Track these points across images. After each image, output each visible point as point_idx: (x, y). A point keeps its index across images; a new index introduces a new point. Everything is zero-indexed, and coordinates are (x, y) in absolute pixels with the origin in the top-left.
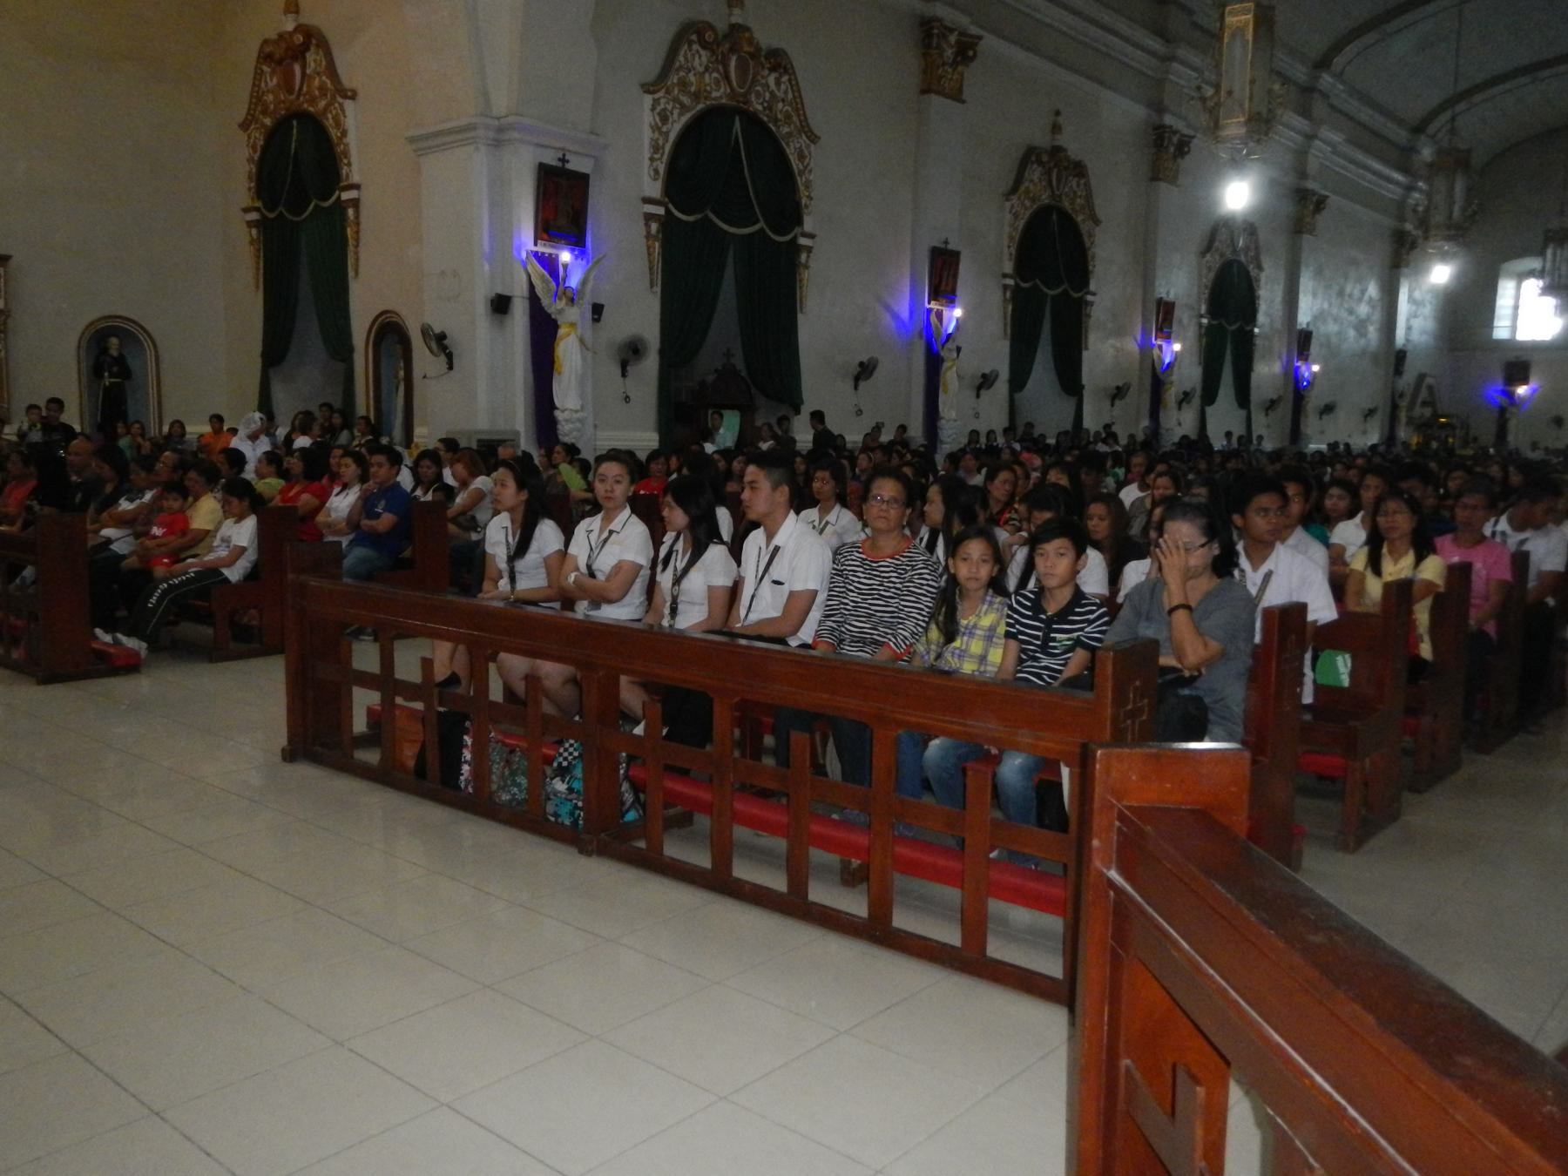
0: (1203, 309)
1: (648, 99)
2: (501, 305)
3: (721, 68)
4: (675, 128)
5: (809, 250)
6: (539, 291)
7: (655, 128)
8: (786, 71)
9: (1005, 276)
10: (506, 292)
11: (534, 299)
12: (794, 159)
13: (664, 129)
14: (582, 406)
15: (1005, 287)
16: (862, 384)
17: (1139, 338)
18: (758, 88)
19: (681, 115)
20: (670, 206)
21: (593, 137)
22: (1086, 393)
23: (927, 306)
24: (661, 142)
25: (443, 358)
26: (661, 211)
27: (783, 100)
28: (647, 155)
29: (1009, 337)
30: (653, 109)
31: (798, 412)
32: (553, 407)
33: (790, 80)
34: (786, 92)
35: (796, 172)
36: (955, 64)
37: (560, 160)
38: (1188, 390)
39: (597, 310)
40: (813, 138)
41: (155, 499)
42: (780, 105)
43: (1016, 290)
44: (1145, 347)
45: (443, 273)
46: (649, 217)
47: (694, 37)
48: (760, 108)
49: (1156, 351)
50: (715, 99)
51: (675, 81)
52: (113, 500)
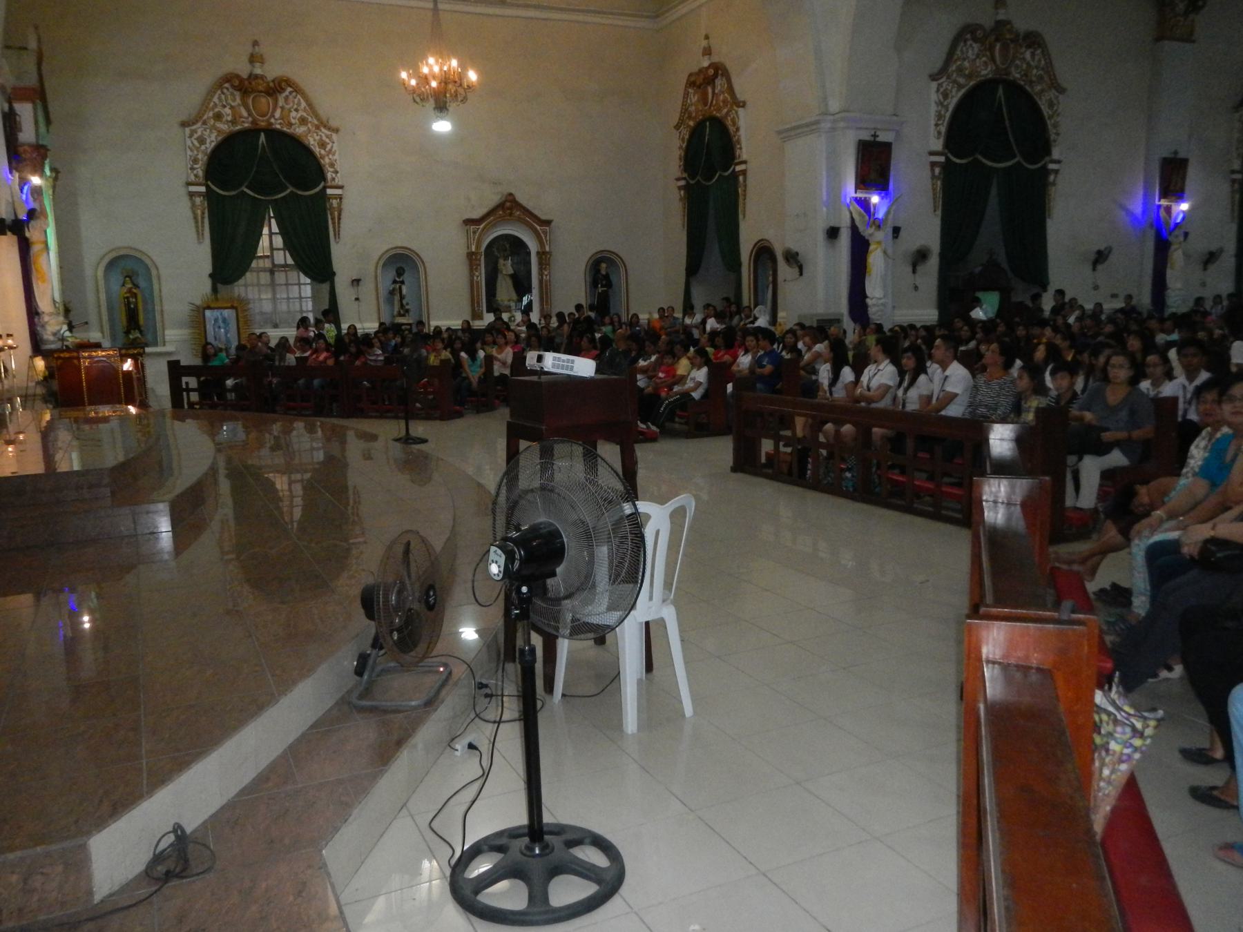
1: (934, 85)
2: (833, 233)
3: (988, 53)
4: (953, 102)
6: (858, 223)
7: (940, 103)
8: (1039, 46)
9: (1233, 172)
10: (837, 225)
11: (854, 228)
13: (945, 103)
14: (884, 296)
15: (1234, 181)
19: (958, 90)
20: (949, 155)
21: (895, 118)
23: (1157, 203)
24: (943, 112)
25: (797, 270)
26: (942, 159)
27: (1037, 67)
28: (933, 122)
30: (938, 90)
31: (1045, 290)
32: (865, 296)
33: (1043, 52)
34: (1040, 61)
35: (1047, 118)
36: (1186, 14)
37: (872, 136)
39: (896, 231)
40: (1061, 90)
42: (1035, 71)
45: (797, 215)
46: (933, 164)
47: (968, 36)
48: (1018, 76)
50: (983, 76)
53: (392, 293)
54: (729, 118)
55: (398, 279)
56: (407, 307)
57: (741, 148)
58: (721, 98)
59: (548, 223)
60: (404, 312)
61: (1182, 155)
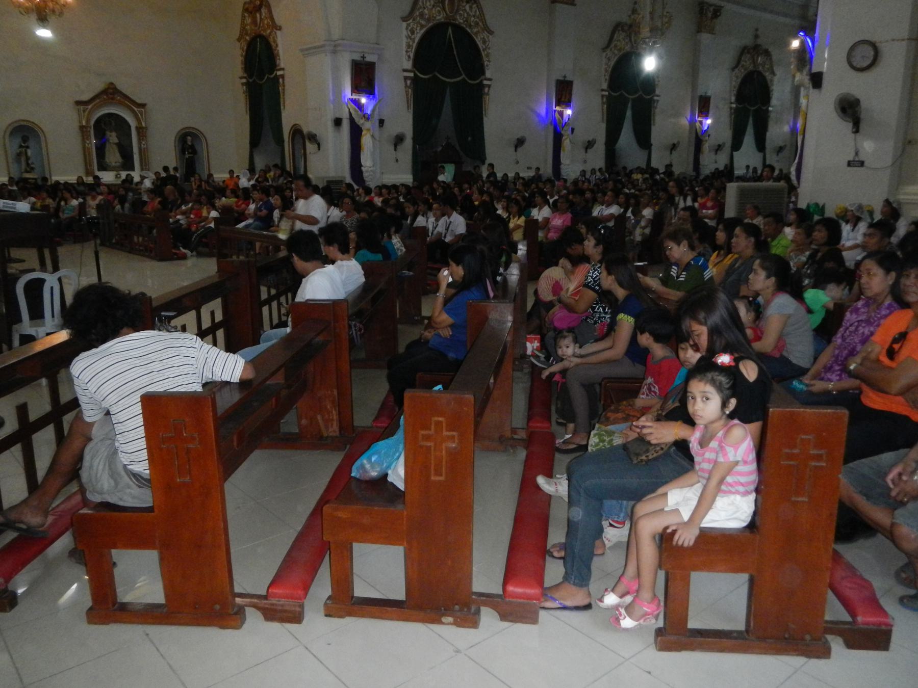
0: (733, 99)
1: (404, 24)
2: (338, 122)
3: (441, 5)
4: (418, 37)
5: (489, 86)
6: (354, 116)
7: (408, 37)
9: (603, 90)
11: (352, 120)
12: (480, 45)
13: (413, 37)
14: (373, 166)
15: (603, 96)
16: (519, 149)
17: (689, 117)
18: (461, 12)
19: (421, 29)
20: (417, 72)
21: (377, 46)
22: (653, 148)
23: (554, 108)
24: (411, 43)
26: (412, 75)
27: (474, 16)
28: (405, 49)
29: (605, 121)
30: (407, 29)
33: (477, 6)
34: (476, 11)
35: (481, 49)
38: (721, 144)
39: (381, 122)
40: (491, 32)
41: (192, 206)
42: (473, 19)
43: (609, 97)
44: (692, 122)
46: (406, 78)
48: (461, 21)
49: (698, 124)
50: (438, 20)
51: (418, 14)
52: (180, 206)
53: (19, 155)
54: (271, 37)
55: (23, 145)
56: (32, 166)
57: (279, 59)
58: (266, 22)
59: (143, 106)
60: (30, 169)
61: (568, 79)
